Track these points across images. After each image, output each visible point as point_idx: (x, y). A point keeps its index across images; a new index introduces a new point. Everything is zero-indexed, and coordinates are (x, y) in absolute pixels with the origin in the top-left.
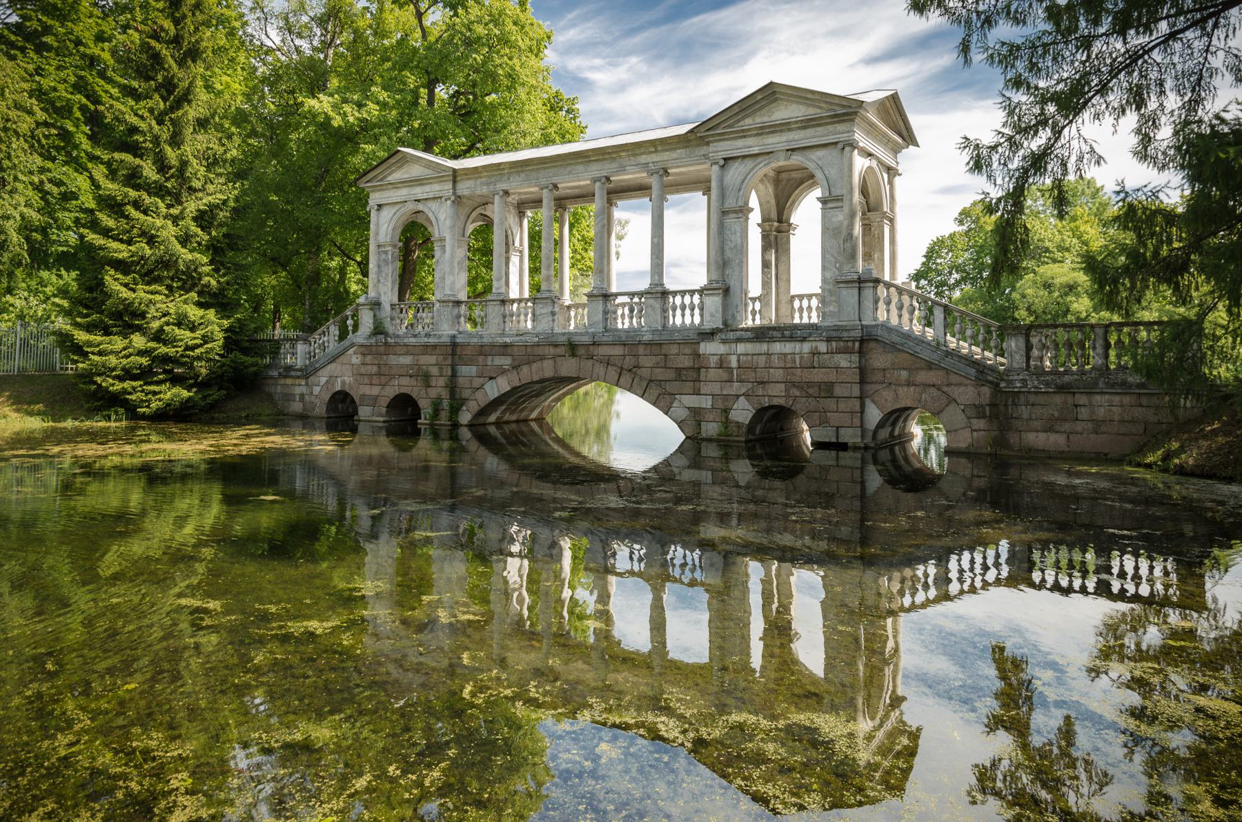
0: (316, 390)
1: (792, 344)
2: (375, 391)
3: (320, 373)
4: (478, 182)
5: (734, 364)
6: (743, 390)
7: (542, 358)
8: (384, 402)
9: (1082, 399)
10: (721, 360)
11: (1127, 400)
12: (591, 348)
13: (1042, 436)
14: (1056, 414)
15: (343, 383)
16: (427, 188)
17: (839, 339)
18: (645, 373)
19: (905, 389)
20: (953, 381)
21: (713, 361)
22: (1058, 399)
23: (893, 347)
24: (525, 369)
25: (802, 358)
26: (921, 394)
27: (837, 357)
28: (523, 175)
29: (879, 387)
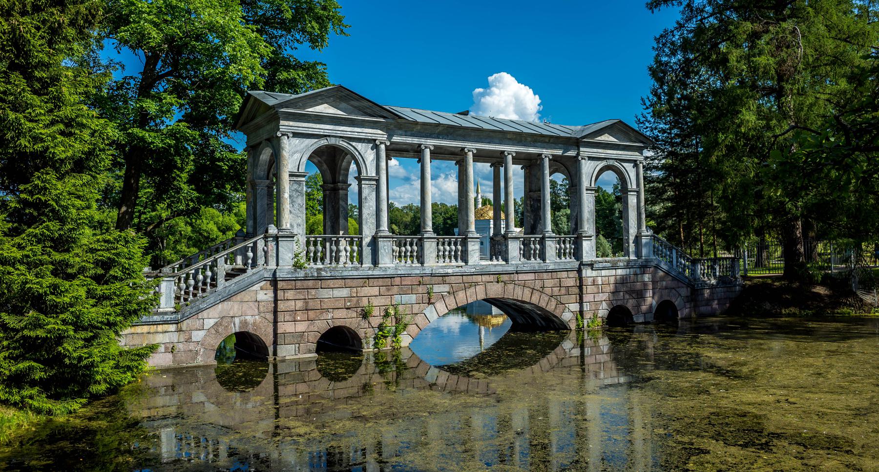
0: (198, 336)
2: (301, 327)
3: (205, 314)
5: (600, 283)
7: (476, 284)
8: (314, 337)
11: (725, 289)
13: (705, 308)
15: (244, 323)
18: (548, 291)
21: (590, 280)
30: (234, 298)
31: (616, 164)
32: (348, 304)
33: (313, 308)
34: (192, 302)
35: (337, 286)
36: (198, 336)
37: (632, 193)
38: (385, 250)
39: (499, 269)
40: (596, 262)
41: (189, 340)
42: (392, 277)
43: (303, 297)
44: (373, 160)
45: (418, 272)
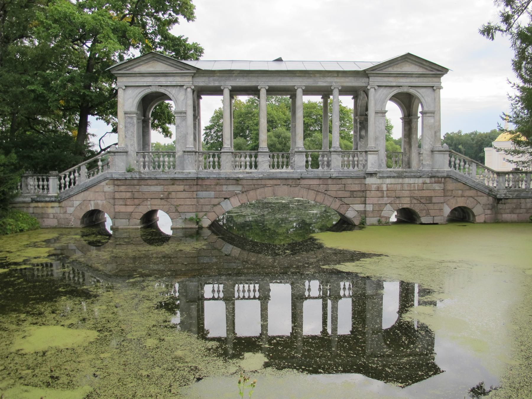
0: (70, 210)
1: (414, 179)
2: (130, 209)
3: (74, 198)
4: (211, 79)
6: (389, 201)
7: (265, 186)
9: (523, 201)
10: (378, 188)
12: (298, 181)
13: (509, 215)
14: (514, 207)
15: (96, 204)
16: (171, 79)
17: (434, 177)
19: (460, 198)
20: (479, 195)
21: (374, 187)
22: (515, 201)
23: (457, 180)
24: (252, 193)
25: (418, 186)
26: (467, 200)
27: (434, 185)
28: (245, 78)
29: (449, 198)
30: (90, 189)
31: (412, 91)
32: (162, 196)
33: (137, 197)
34: (67, 190)
35: (153, 184)
36: (70, 210)
37: (428, 115)
38: (189, 160)
39: (286, 176)
40: (379, 172)
41: (65, 212)
42: (192, 179)
43: (130, 190)
44: (184, 100)
45: (215, 176)
